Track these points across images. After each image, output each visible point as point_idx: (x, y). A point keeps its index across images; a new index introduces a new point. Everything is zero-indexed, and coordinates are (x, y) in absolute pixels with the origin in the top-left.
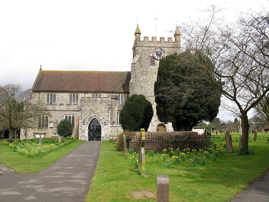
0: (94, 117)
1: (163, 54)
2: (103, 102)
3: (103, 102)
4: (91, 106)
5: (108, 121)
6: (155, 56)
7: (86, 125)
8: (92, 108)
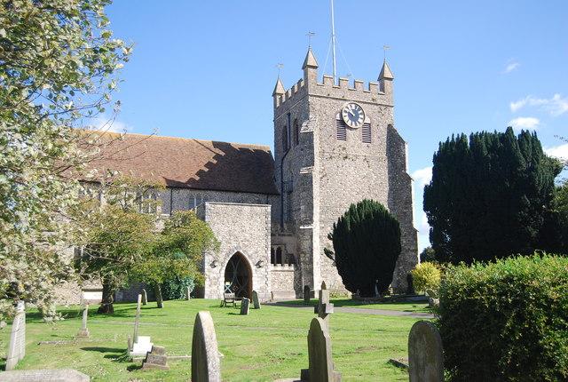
1: (361, 116)
6: (346, 119)
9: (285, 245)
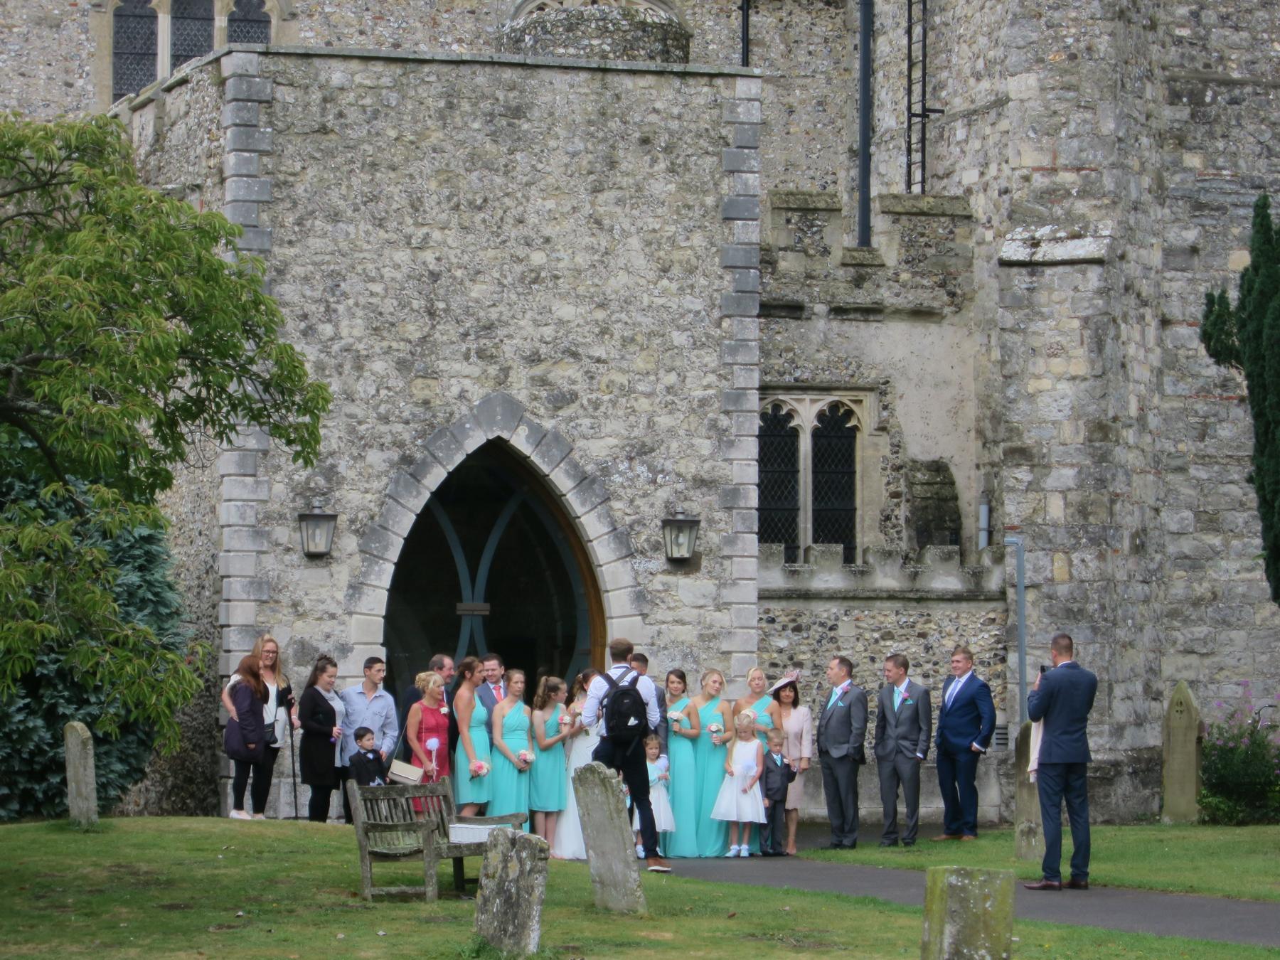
0: (483, 413)
2: (630, 160)
3: (630, 160)
4: (435, 210)
5: (731, 497)
7: (342, 573)
8: (449, 245)
9: (881, 389)
